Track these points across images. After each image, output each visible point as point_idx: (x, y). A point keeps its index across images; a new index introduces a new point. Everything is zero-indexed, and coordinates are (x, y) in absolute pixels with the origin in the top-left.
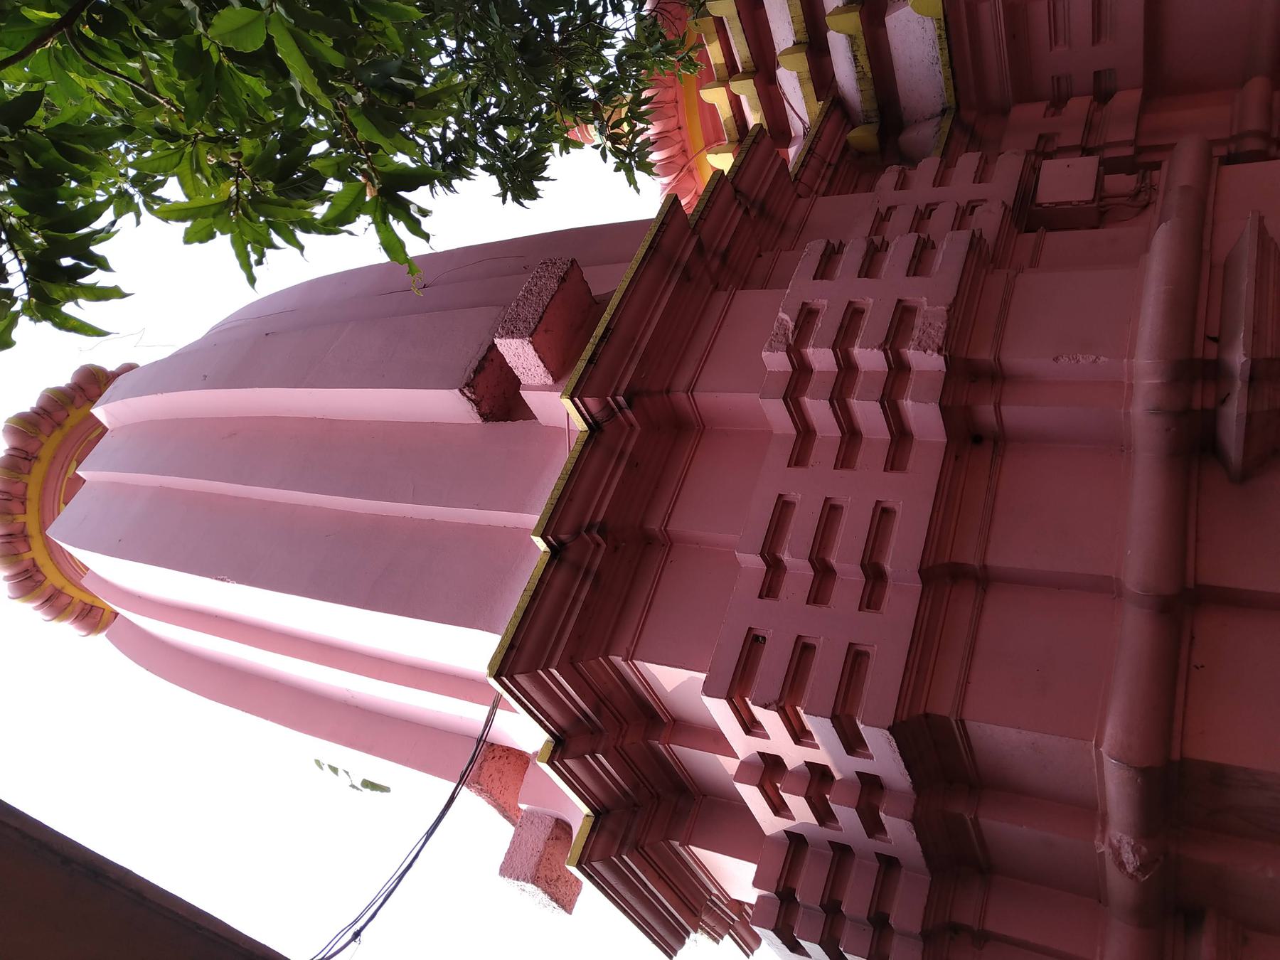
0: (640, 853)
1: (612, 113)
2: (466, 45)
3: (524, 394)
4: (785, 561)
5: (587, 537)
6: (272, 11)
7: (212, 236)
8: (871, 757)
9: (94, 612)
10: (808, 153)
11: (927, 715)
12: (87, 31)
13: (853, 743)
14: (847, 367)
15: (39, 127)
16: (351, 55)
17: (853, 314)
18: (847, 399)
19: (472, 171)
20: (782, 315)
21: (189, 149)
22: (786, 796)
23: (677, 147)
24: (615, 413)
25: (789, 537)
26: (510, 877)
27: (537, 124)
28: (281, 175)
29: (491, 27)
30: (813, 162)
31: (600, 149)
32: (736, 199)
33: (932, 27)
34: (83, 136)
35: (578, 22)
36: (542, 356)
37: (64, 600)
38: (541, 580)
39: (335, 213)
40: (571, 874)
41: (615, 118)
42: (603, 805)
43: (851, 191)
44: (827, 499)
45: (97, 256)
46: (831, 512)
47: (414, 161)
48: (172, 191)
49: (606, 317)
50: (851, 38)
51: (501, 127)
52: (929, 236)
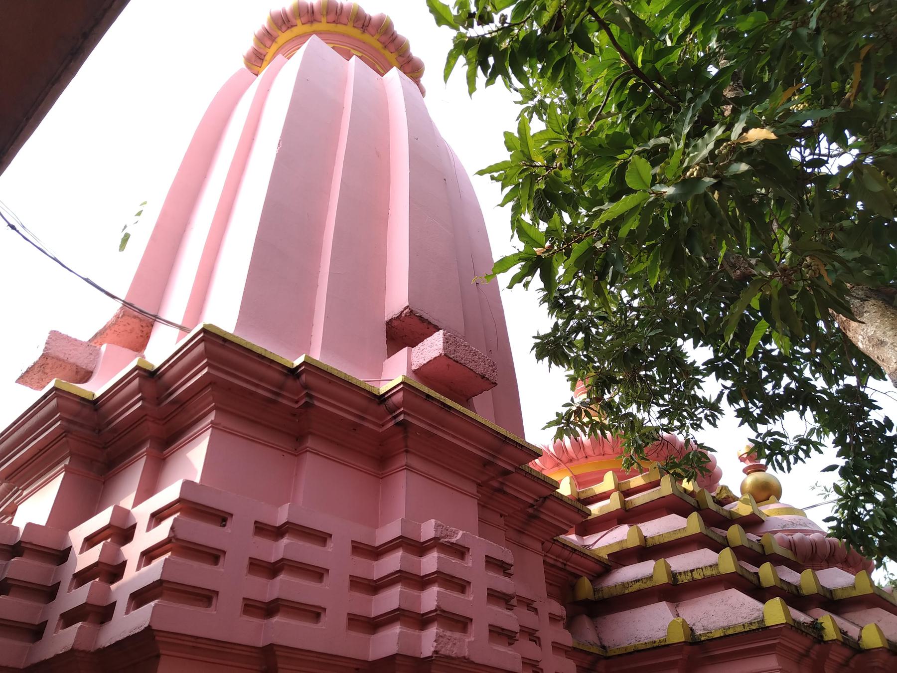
0: (62, 434)
1: (596, 411)
2: (635, 313)
3: (405, 349)
4: (282, 540)
5: (303, 394)
6: (651, 194)
7: (509, 149)
8: (127, 612)
9: (259, 60)
10: (572, 548)
11: (158, 656)
12: (632, 82)
13: (139, 598)
14: (423, 582)
15: (573, 50)
16: (626, 240)
17: (462, 586)
18: (400, 584)
19: (554, 316)
20: (461, 533)
21: (563, 137)
22: (100, 546)
23: (574, 456)
24: (391, 413)
25: (301, 543)
26: (49, 338)
27: (586, 360)
28: (547, 194)
29: (648, 330)
30: (566, 553)
31: (571, 402)
32: (540, 498)
33: (659, 637)
34: (569, 75)
35: (653, 388)
36: (431, 362)
37: (268, 43)
38: (272, 361)
39: (526, 228)
40: (48, 383)
41: (592, 412)
42: (101, 407)
43: (547, 580)
44: (327, 571)
45: (495, 79)
46: (318, 574)
47: (559, 278)
48: (537, 125)
49: (458, 407)
50: (651, 577)
51: (583, 335)
52: (517, 640)
